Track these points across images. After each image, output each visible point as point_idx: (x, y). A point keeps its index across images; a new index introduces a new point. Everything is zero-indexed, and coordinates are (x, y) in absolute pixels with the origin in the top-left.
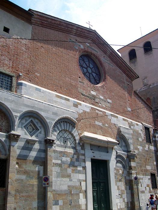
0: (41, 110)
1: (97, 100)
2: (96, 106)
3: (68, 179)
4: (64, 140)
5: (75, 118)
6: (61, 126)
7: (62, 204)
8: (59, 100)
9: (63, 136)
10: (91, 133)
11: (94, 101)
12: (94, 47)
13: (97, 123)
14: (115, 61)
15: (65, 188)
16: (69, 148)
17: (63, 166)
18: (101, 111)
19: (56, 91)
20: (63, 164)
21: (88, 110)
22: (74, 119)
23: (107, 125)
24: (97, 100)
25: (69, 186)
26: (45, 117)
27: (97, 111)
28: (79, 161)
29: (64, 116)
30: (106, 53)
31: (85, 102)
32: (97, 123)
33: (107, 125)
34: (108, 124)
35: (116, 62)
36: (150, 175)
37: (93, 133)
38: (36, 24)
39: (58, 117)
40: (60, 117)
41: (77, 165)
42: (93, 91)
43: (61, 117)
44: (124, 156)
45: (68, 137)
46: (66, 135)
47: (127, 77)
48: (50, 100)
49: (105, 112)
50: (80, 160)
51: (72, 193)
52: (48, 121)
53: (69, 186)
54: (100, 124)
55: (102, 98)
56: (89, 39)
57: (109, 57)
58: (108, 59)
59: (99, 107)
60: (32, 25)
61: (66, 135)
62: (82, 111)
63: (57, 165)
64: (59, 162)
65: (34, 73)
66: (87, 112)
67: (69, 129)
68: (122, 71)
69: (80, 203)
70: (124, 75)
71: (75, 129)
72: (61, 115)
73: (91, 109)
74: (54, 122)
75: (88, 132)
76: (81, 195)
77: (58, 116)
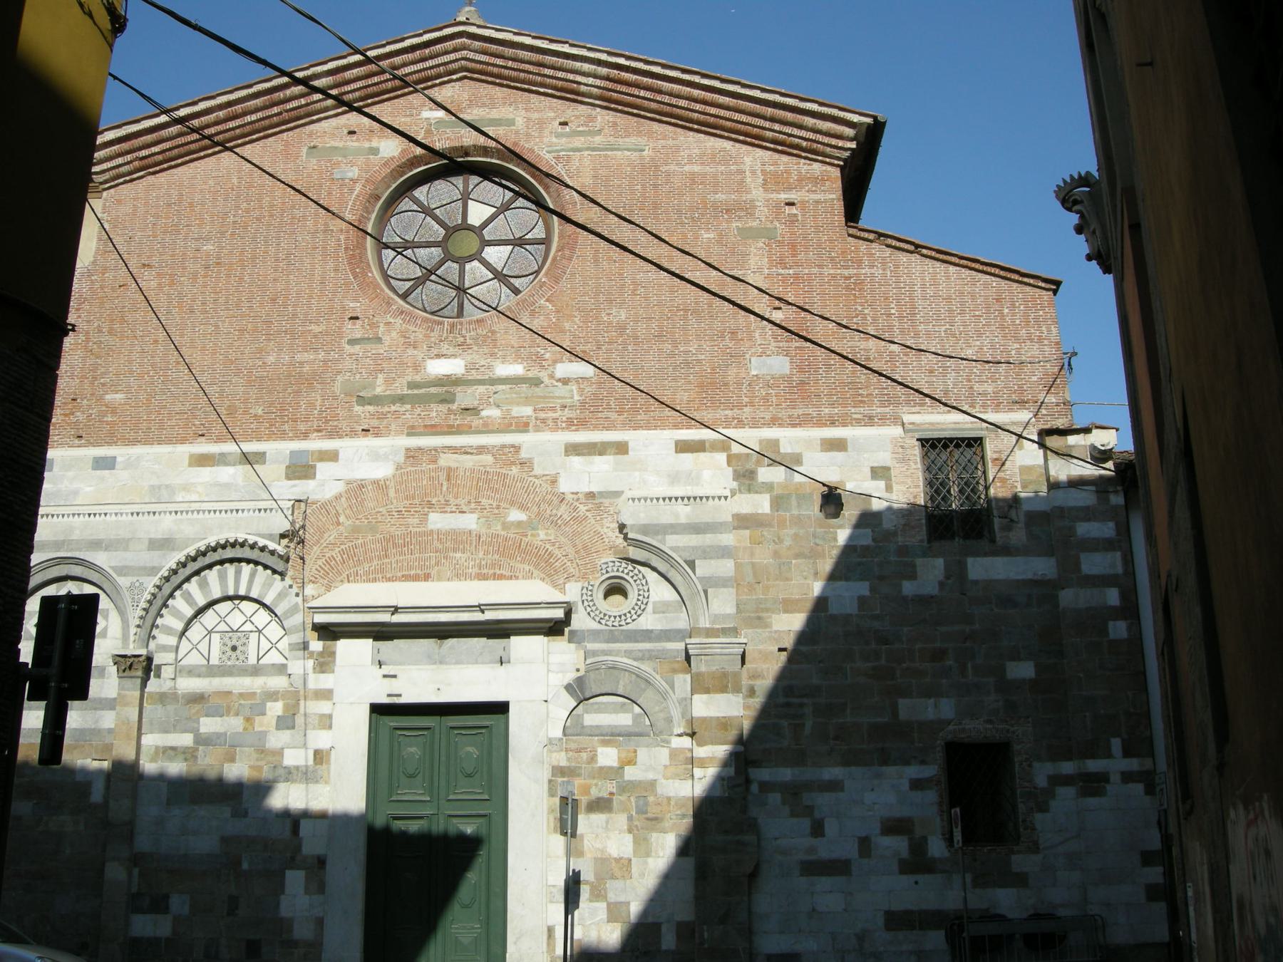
0: (96, 545)
1: (466, 397)
2: (469, 430)
3: (226, 811)
4: (225, 645)
5: (270, 537)
6: (204, 585)
7: (186, 910)
8: (206, 474)
9: (223, 627)
10: (389, 580)
11: (443, 408)
12: (484, 105)
13: (437, 521)
14: (653, 105)
15: (205, 844)
16: (251, 676)
17: (200, 753)
18: (481, 450)
19: (203, 435)
20: (201, 748)
21: (382, 471)
22: (261, 542)
23: (516, 515)
24: (466, 397)
25: (224, 840)
26: (110, 567)
27: (446, 460)
28: (293, 728)
29: (206, 542)
30: (578, 93)
31: (377, 435)
32: (437, 521)
33: (516, 515)
34: (523, 507)
35: (668, 109)
36: (939, 755)
37: (407, 578)
38: (121, 180)
39: (175, 554)
40: (185, 552)
41: (280, 746)
42: (438, 356)
43: (191, 551)
44: (646, 667)
45: (248, 627)
46: (236, 620)
47: (785, 158)
48: (159, 487)
49: (516, 448)
50: (299, 720)
51: (245, 866)
52: (123, 582)
53: (224, 840)
54: (469, 522)
55: (516, 369)
56: (441, 84)
57: (609, 102)
58: (603, 117)
59: (487, 429)
60: (105, 194)
61: (236, 620)
62: (340, 487)
63: (172, 753)
64: (186, 740)
65: (101, 398)
66: (376, 482)
67: (249, 588)
68: (728, 145)
69: (285, 910)
70: (753, 159)
71: (288, 581)
72: (195, 540)
73: (402, 460)
74: (156, 580)
75: (369, 581)
76: (295, 879)
77: (173, 549)
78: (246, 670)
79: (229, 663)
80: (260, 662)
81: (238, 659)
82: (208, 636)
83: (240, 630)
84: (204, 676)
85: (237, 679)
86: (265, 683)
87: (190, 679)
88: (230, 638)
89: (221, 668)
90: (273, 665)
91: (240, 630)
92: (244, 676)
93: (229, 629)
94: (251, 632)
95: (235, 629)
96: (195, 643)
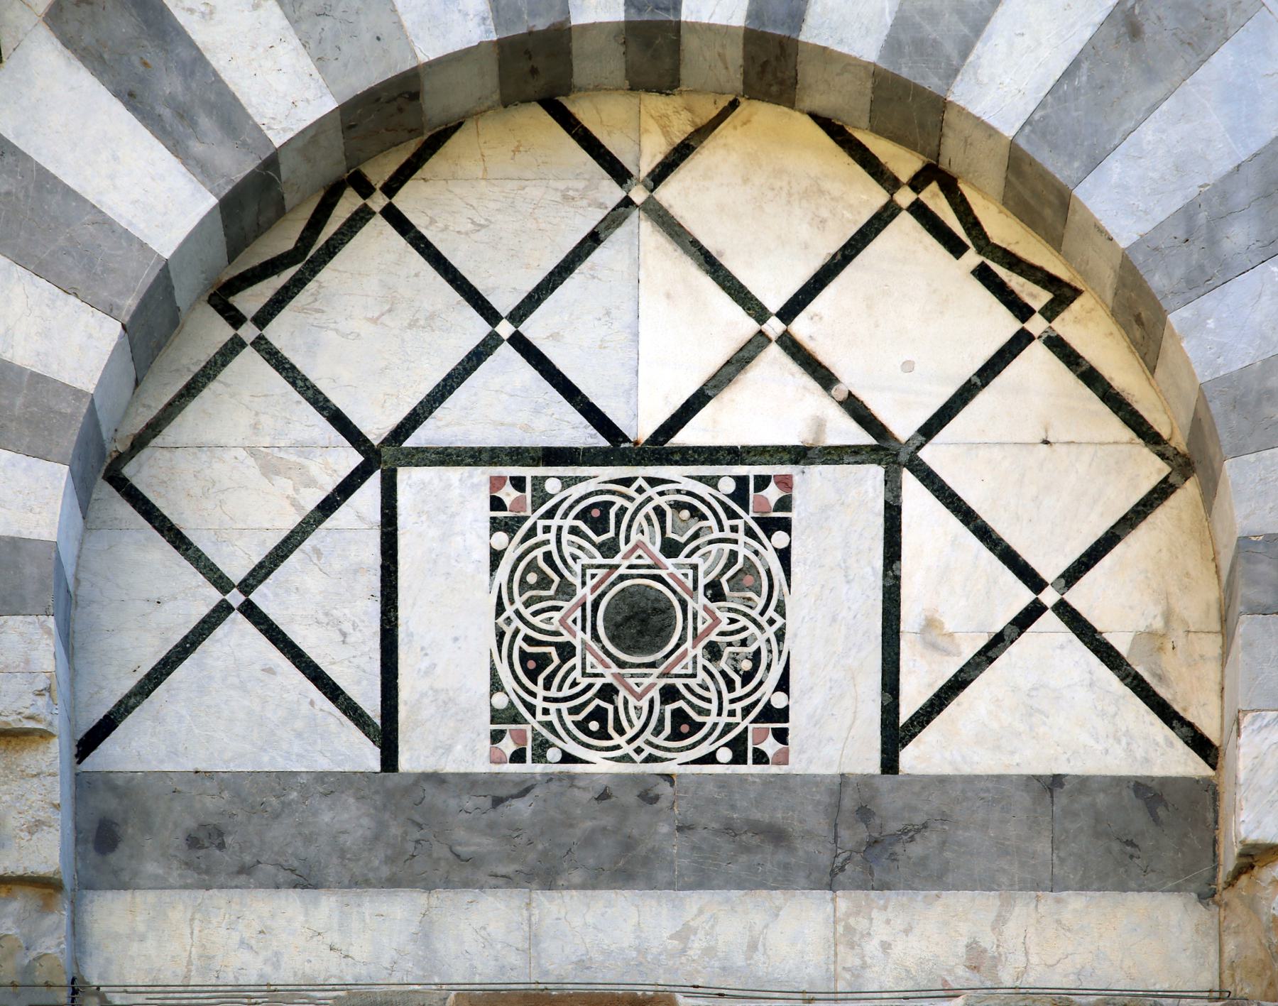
16: (831, 880)
78: (777, 836)
79: (599, 764)
80: (911, 758)
81: (683, 726)
82: (372, 488)
83: (689, 436)
84: (360, 882)
85: (695, 901)
86: (976, 958)
87: (219, 901)
88: (596, 517)
89: (522, 808)
90: (1056, 781)
91: (689, 436)
92: (752, 881)
93: (583, 435)
94: (800, 455)
95: (642, 428)
96: (236, 568)
